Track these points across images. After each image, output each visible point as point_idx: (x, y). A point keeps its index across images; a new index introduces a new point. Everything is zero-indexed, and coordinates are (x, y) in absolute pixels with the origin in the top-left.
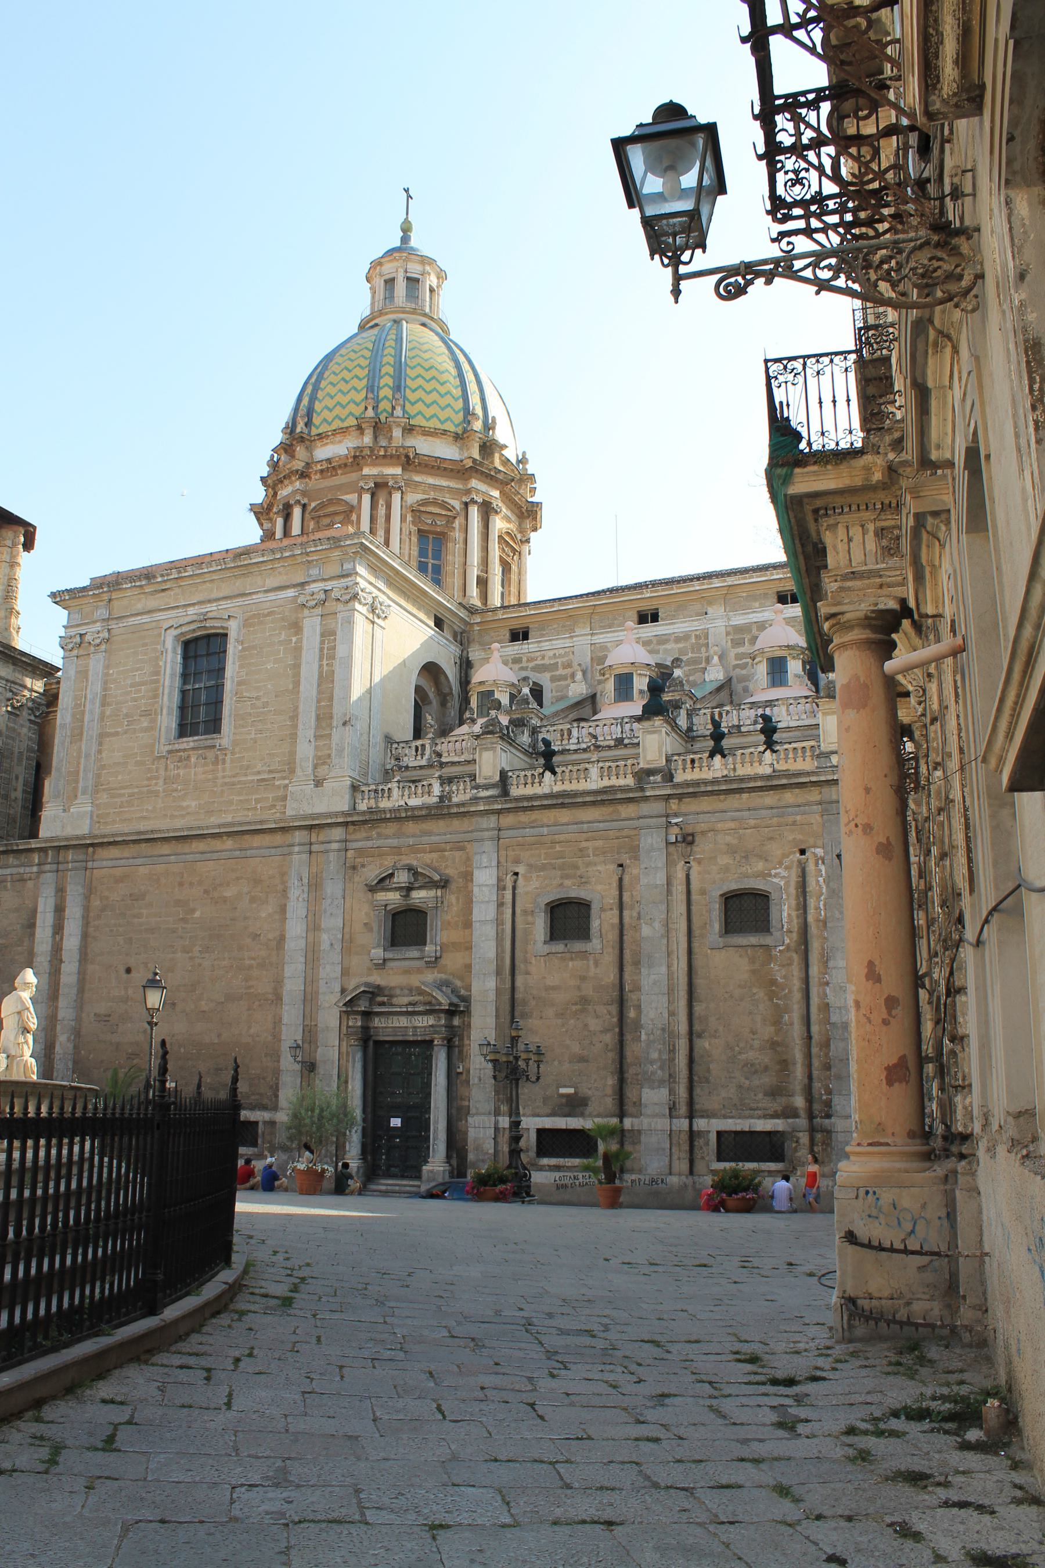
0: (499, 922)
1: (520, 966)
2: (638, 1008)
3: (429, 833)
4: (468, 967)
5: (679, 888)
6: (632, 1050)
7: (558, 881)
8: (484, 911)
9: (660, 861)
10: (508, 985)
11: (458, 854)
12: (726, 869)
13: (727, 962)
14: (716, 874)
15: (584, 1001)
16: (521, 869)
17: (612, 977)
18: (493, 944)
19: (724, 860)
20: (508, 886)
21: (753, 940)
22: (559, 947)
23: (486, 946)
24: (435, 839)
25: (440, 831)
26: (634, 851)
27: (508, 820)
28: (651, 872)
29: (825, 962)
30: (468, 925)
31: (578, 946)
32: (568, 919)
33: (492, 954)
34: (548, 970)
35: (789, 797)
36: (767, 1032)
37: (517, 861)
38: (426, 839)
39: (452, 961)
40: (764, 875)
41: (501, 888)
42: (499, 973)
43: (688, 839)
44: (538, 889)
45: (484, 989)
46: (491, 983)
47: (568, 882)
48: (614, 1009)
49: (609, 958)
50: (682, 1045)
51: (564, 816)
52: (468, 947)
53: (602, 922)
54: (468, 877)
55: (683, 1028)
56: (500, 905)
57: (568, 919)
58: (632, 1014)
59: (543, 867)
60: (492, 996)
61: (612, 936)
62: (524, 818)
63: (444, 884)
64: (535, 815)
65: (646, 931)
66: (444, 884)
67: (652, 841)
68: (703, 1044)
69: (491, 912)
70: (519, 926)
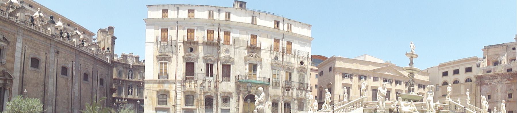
0: (21, 59)
1: (25, 71)
2: (48, 87)
3: (7, 27)
4: (13, 69)
5: (56, 63)
6: (46, 97)
7: (34, 52)
8: (18, 54)
9: (54, 56)
10: (22, 76)
11: (13, 36)
12: (63, 61)
13: (62, 80)
14: (62, 62)
15: (37, 83)
16: (27, 46)
17: (43, 79)
18: (19, 64)
19: (63, 59)
20: (24, 49)
21: (66, 77)
22: (33, 69)
23: (18, 65)
24: (7, 29)
25: (9, 28)
26: (49, 51)
27: (26, 33)
28: (52, 57)
29: (74, 84)
30: (13, 56)
31: (37, 70)
32: (35, 62)
33: (19, 66)
34: (31, 74)
35: (72, 50)
36: (67, 96)
37: (26, 44)
38: (5, 28)
39: (9, 66)
40: (67, 64)
41: (22, 50)
42: (20, 72)
43: (58, 53)
44: (30, 53)
45: (16, 75)
46: (18, 75)
47: (36, 53)
48: (43, 87)
49: (43, 74)
50: (54, 97)
51: (37, 37)
52: (13, 63)
53: (42, 65)
54: (15, 43)
55: (55, 93)
56: (22, 54)
57: (35, 62)
58: (46, 88)
59: (32, 48)
60: (18, 78)
61: (44, 69)
62: (29, 34)
63: (8, 43)
64: (31, 34)
65: (50, 70)
66: (8, 43)
67: (52, 50)
68: (58, 97)
69: (20, 56)
70: (25, 61)
